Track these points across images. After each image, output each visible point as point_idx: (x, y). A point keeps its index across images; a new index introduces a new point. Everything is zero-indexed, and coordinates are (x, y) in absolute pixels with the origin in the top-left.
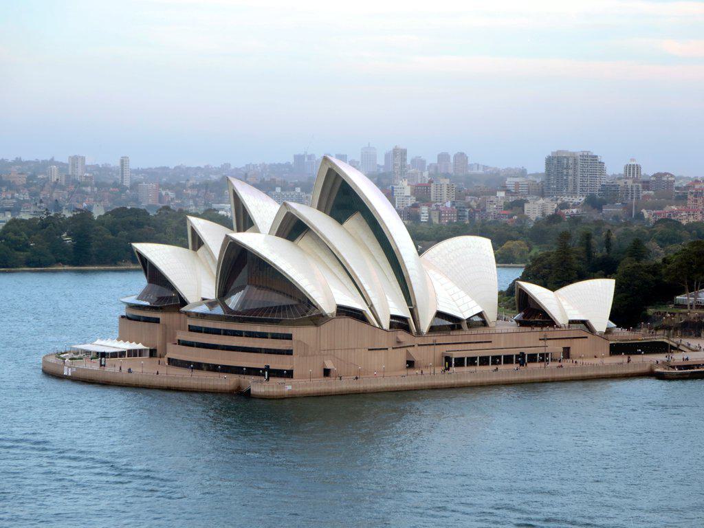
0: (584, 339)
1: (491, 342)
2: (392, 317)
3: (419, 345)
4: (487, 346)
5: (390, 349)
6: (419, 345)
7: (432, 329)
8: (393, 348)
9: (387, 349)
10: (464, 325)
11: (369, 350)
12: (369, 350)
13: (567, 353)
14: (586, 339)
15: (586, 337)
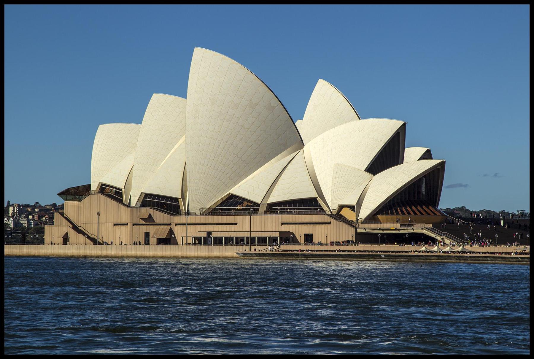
0: (327, 225)
1: (236, 224)
2: (147, 195)
3: (176, 225)
4: (233, 228)
5: (129, 224)
6: (176, 225)
7: (213, 211)
8: (134, 225)
9: (127, 224)
10: (263, 209)
11: (115, 225)
12: (115, 225)
13: (309, 239)
14: (329, 225)
15: (330, 223)
